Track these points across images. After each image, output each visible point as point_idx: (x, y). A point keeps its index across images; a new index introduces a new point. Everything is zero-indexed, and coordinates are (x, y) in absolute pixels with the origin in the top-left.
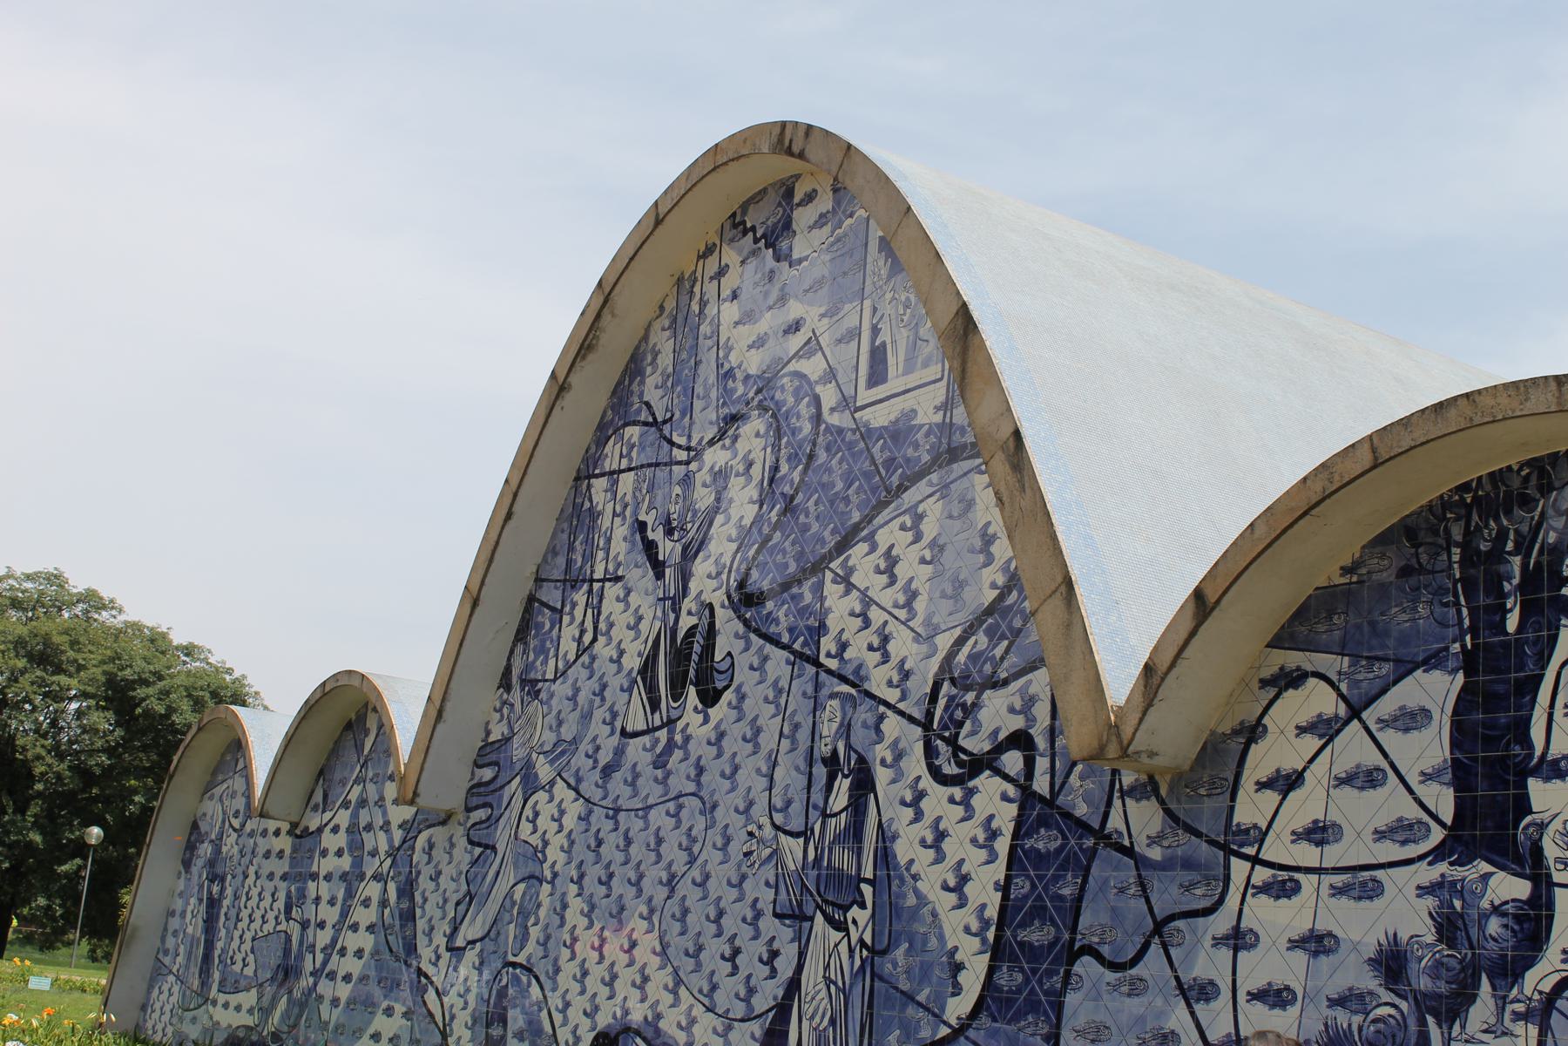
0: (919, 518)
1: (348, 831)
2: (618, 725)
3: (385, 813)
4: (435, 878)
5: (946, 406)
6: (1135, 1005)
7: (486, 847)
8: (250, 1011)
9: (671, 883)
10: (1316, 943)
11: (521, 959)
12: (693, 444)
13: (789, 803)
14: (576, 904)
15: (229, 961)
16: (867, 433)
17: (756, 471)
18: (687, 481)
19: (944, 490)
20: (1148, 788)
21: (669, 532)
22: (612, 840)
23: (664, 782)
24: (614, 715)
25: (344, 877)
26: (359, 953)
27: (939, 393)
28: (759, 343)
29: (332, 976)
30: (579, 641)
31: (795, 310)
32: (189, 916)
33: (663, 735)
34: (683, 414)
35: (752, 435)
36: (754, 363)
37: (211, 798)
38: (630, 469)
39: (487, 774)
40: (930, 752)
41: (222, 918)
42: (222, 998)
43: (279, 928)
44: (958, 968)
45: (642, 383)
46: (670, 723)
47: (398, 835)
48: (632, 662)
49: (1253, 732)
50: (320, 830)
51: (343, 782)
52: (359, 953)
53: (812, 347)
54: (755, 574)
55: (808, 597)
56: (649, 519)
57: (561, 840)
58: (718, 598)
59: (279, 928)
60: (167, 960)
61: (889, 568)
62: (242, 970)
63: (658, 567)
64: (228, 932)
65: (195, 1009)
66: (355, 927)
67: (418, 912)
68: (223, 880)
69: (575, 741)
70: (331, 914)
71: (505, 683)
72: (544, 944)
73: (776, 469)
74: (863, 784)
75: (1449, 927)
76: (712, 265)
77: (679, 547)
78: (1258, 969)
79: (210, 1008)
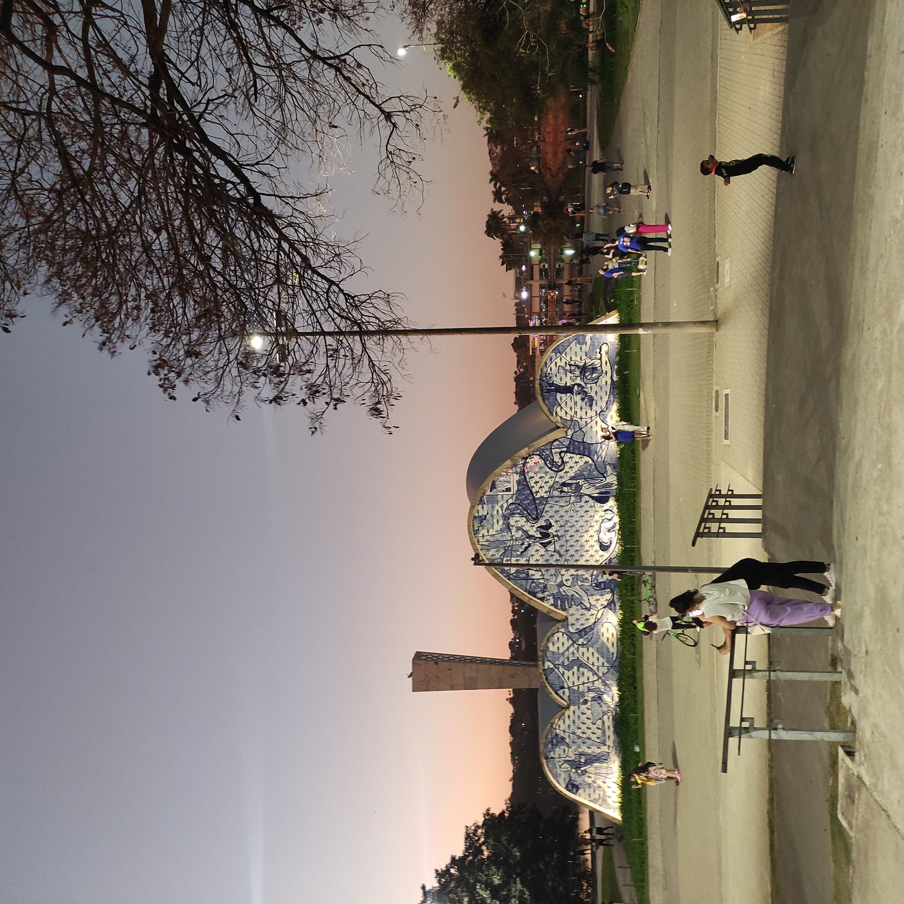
0: (532, 477)
1: (569, 671)
3: (565, 651)
4: (577, 619)
5: (516, 473)
6: (588, 433)
7: (572, 599)
8: (609, 718)
10: (581, 408)
11: (590, 578)
12: (510, 538)
13: (566, 502)
16: (518, 491)
17: (518, 519)
18: (516, 540)
19: (528, 472)
20: (566, 432)
21: (523, 544)
23: (562, 536)
24: (552, 555)
25: (578, 670)
27: (515, 475)
28: (498, 521)
31: (495, 512)
32: (589, 781)
33: (556, 538)
34: (505, 543)
35: (512, 521)
36: (501, 522)
38: (510, 560)
39: (559, 602)
41: (589, 751)
44: (586, 462)
46: (554, 536)
47: (571, 642)
48: (542, 551)
49: (561, 417)
50: (569, 688)
51: (559, 677)
53: (502, 507)
54: (534, 516)
56: (521, 550)
58: (536, 526)
61: (536, 482)
63: (529, 545)
66: (588, 658)
67: (584, 627)
68: (581, 754)
70: (585, 670)
71: (542, 599)
73: (519, 514)
75: (579, 394)
76: (481, 539)
77: (527, 540)
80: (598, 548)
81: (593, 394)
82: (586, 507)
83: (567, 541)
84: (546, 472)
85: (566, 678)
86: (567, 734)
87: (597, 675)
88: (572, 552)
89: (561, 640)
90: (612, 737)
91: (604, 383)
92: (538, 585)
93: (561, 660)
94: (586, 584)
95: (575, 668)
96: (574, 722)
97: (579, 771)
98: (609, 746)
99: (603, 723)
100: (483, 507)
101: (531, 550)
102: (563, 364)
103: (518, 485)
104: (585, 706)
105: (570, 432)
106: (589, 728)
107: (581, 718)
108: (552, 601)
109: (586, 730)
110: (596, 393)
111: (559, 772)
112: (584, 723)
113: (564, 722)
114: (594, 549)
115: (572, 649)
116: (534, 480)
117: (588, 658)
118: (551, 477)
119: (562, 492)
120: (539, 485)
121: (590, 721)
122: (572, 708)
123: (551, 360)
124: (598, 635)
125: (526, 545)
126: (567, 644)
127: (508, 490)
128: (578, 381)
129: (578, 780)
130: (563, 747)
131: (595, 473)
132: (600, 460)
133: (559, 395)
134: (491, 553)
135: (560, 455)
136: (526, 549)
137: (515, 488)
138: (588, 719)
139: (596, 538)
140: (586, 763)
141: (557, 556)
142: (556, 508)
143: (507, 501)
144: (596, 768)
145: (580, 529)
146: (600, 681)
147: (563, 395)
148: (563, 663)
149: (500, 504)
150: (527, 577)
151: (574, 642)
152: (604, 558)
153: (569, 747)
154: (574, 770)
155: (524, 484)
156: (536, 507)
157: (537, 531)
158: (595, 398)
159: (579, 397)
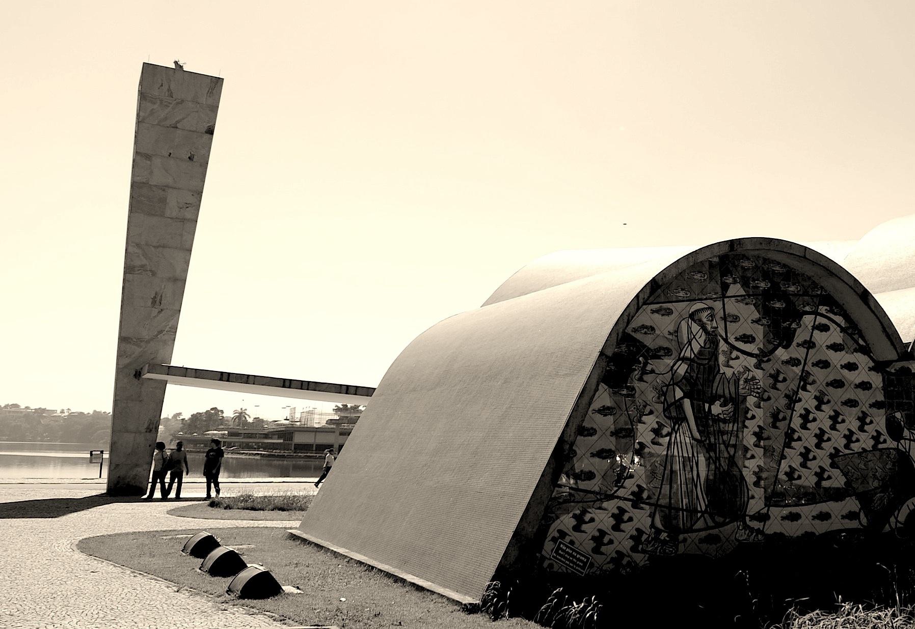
8: (852, 516)
15: (782, 477)
32: (644, 433)
37: (669, 312)
42: (775, 512)
43: (880, 446)
59: (880, 446)
60: (594, 485)
62: (818, 484)
64: (768, 452)
65: (708, 528)
68: (737, 401)
79: (755, 525)
86: (800, 353)
90: (793, 529)
96: (838, 384)
97: (679, 394)
99: (837, 495)
104: (883, 430)
106: (820, 437)
107: (846, 410)
111: (679, 308)
112: (835, 419)
113: (835, 347)
121: (837, 440)
122: (876, 380)
129: (646, 390)
130: (759, 332)
138: (849, 437)
153: (763, 357)
154: (682, 369)
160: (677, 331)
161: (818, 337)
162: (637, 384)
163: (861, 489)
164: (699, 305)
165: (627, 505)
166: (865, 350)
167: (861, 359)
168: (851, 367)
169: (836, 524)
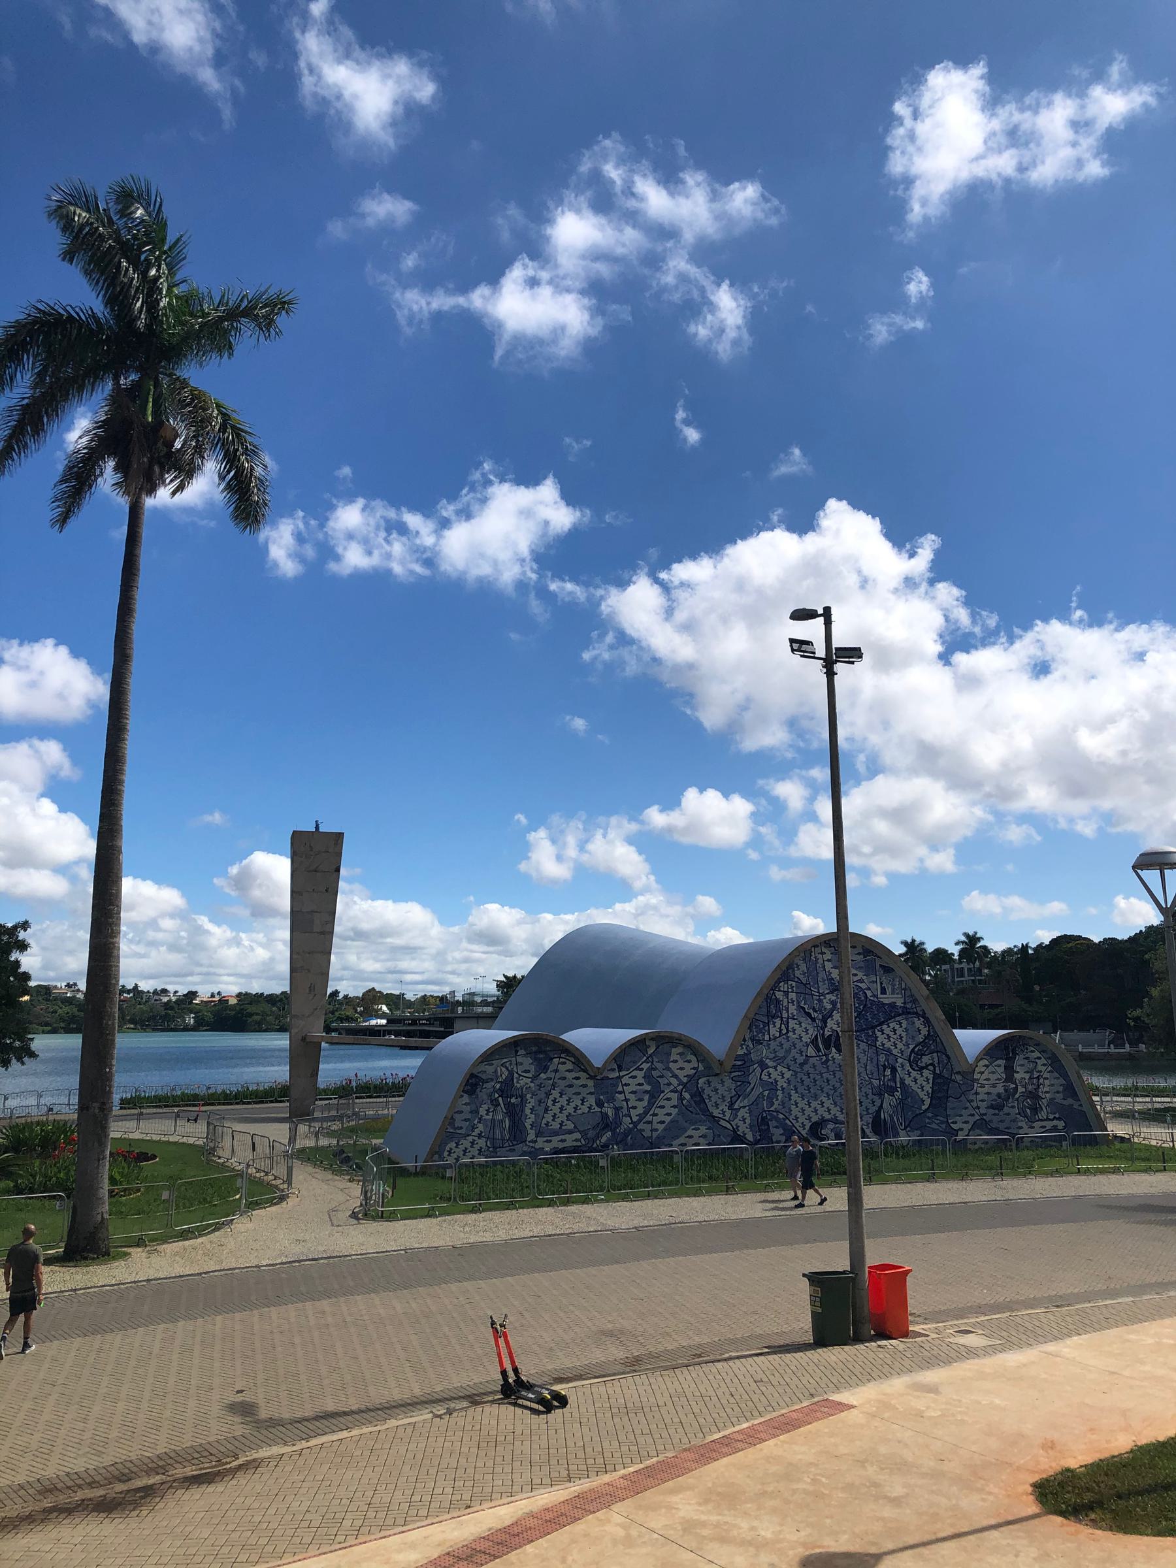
0: (900, 1023)
2: (804, 1054)
3: (672, 1072)
8: (576, 1140)
9: (835, 1089)
10: (988, 1093)
14: (795, 1096)
16: (884, 1004)
18: (820, 1001)
19: (907, 1019)
20: (958, 1073)
21: (815, 1011)
22: (807, 1081)
25: (646, 1092)
26: (669, 1114)
29: (649, 1122)
30: (780, 1032)
32: (482, 1111)
39: (739, 1063)
40: (911, 1066)
41: (528, 1111)
45: (794, 970)
47: (685, 1080)
48: (806, 1039)
50: (620, 1078)
51: (635, 1062)
52: (669, 1114)
53: (861, 981)
55: (870, 1032)
56: (806, 1007)
57: (785, 1080)
61: (895, 1031)
63: (813, 1020)
66: (663, 1107)
67: (707, 1101)
68: (522, 1097)
69: (784, 1058)
70: (645, 1103)
72: (783, 1103)
74: (894, 1070)
75: (1006, 1091)
76: (818, 950)
77: (820, 1017)
78: (979, 1097)
79: (531, 1144)
80: (813, 1120)
81: (1006, 1110)
82: (866, 1103)
83: (821, 1074)
84: (907, 1045)
85: (633, 1074)
87: (640, 1121)
88: (807, 1081)
89: (686, 1065)
91: (1020, 1124)
92: (760, 1031)
93: (659, 1065)
94: (765, 1102)
95: (648, 1088)
96: (571, 1086)
97: (497, 1095)
98: (536, 1141)
99: (570, 1132)
100: (859, 954)
101: (806, 1023)
102: (1040, 1068)
103: (889, 1004)
105: (958, 1078)
106: (561, 1109)
108: (740, 1052)
109: (558, 1105)
110: (1008, 1114)
112: (569, 1101)
113: (569, 1071)
114: (813, 1114)
115: (674, 1082)
116: (897, 1027)
117: (663, 1107)
118: (902, 1052)
119: (885, 1067)
120: (891, 1034)
121: (570, 1109)
122: (591, 1083)
123: (1044, 1051)
124: (696, 1123)
125: (814, 1015)
126: (681, 1074)
127: (883, 991)
128: (1021, 1089)
129: (483, 1095)
130: (532, 1068)
131: (910, 1115)
132: (927, 1121)
133: (1002, 1062)
134: (801, 963)
135: (931, 1064)
136: (809, 1015)
137: (887, 999)
138: (576, 1108)
139: (827, 1116)
140: (509, 1105)
141: (801, 1059)
142: (864, 1059)
143: (869, 989)
144: (502, 1122)
145: (837, 1093)
146: (631, 1126)
147: (1002, 1069)
148: (655, 1069)
149: (864, 977)
150: (771, 1016)
151: (685, 1085)
152: (800, 1129)
153: (534, 1078)
154: (498, 1086)
155: (891, 1013)
156: (863, 1030)
157: (833, 1031)
158: (1001, 1113)
159: (1002, 1090)
160: (496, 1071)
161: (562, 1068)
162: (480, 1094)
163: (581, 1129)
164: (505, 1060)
165: (476, 1138)
166: (585, 1071)
167: (583, 1075)
168: (578, 1078)
169: (569, 1144)
